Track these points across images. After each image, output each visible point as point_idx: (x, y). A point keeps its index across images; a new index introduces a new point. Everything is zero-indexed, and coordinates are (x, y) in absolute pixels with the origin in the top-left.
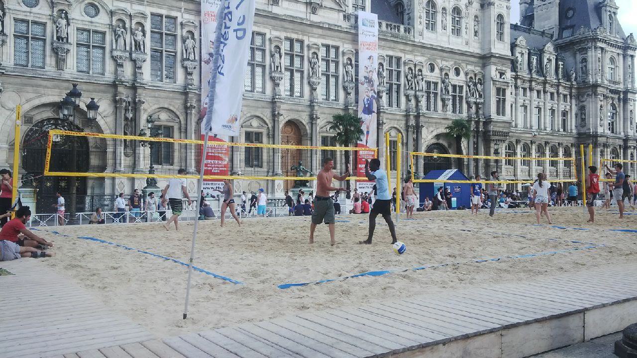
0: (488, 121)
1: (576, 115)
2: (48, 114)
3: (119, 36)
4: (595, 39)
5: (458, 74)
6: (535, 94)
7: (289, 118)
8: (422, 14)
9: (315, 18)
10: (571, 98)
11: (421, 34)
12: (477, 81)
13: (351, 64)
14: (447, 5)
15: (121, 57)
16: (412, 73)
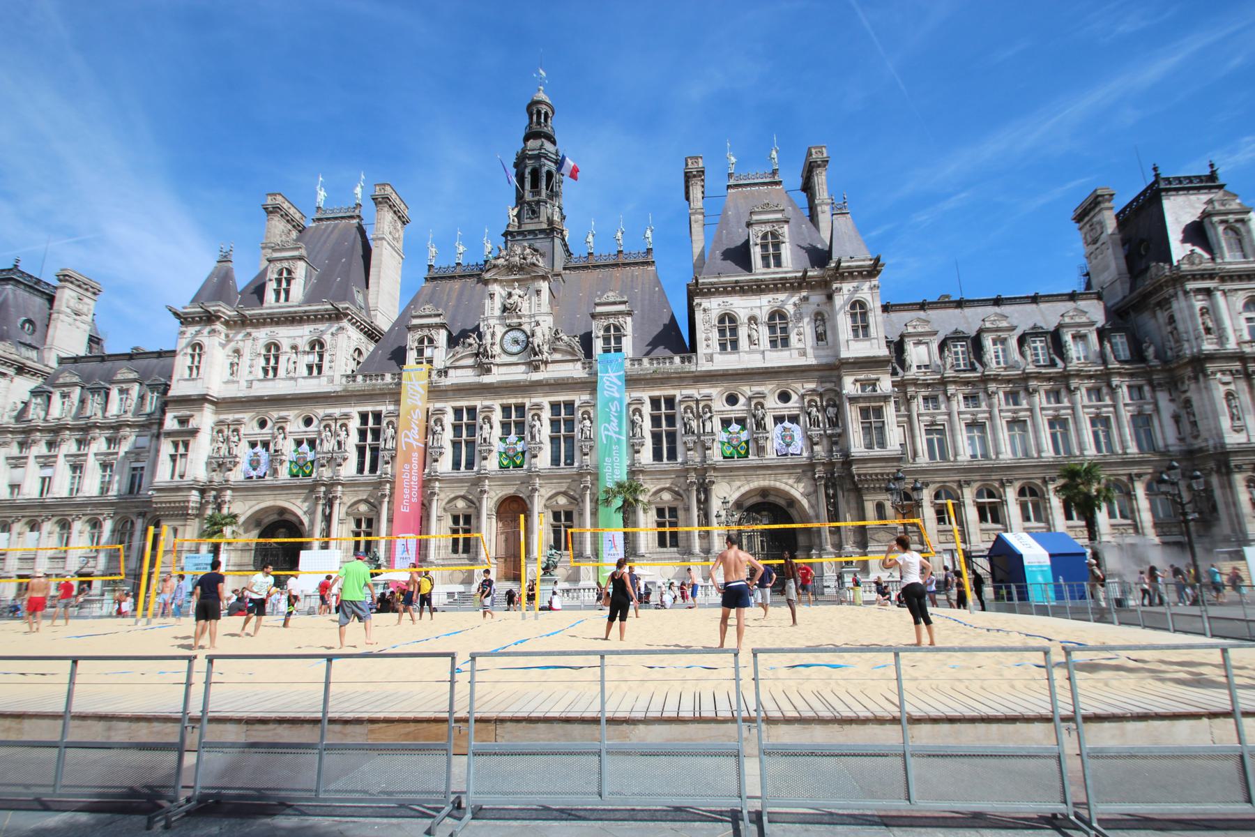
0: (848, 461)
1: (1177, 419)
2: (274, 517)
3: (322, 440)
4: (1179, 279)
5: (785, 397)
6: (1040, 400)
7: (504, 493)
8: (710, 335)
9: (536, 376)
10: (1153, 389)
11: (712, 360)
12: (824, 403)
13: (589, 418)
14: (757, 312)
15: (323, 458)
16: (692, 412)
